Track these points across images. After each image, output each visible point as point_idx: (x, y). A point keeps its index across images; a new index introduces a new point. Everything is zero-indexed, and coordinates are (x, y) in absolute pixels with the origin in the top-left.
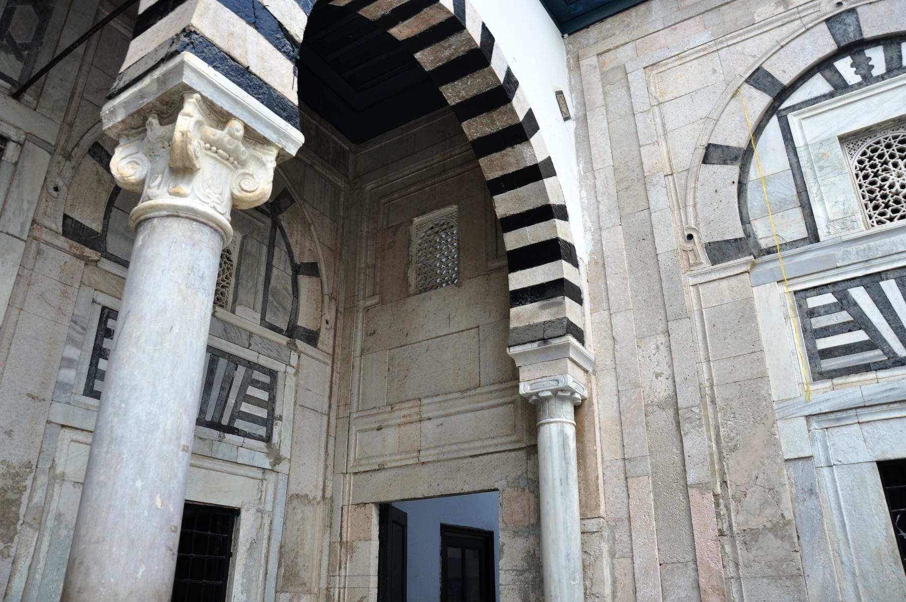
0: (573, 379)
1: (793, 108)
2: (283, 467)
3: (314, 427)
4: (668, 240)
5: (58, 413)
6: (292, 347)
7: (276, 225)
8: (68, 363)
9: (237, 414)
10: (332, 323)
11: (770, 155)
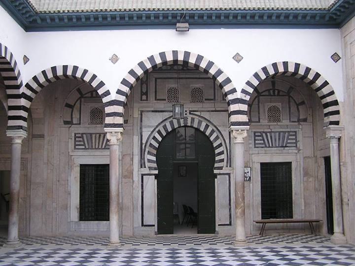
5: (251, 152)
6: (299, 124)
7: (290, 97)
8: (250, 143)
10: (311, 114)
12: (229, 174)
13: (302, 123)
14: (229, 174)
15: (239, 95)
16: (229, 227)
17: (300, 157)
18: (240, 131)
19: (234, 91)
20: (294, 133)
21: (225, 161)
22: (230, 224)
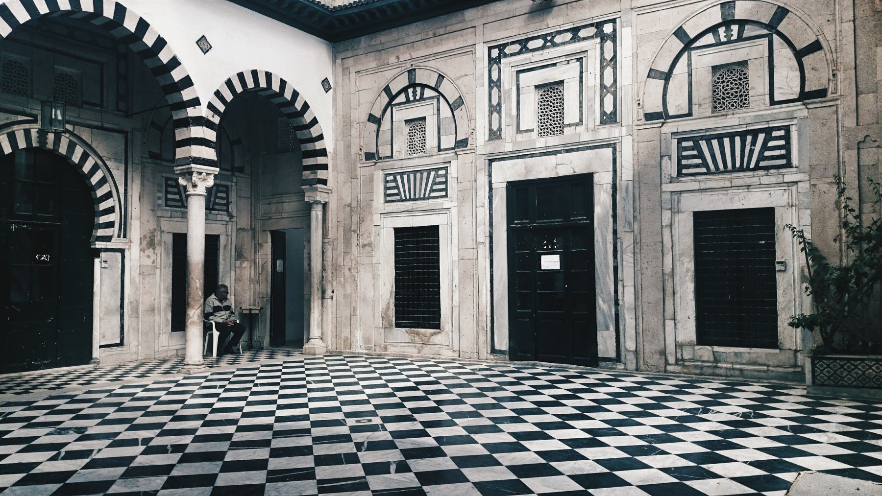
0: (320, 197)
1: (395, 105)
2: (234, 219)
3: (245, 204)
4: (355, 150)
5: (159, 213)
6: (233, 175)
8: (159, 198)
9: (215, 204)
11: (386, 125)
12: (122, 251)
13: (236, 174)
14: (122, 251)
15: (202, 111)
16: (119, 348)
17: (232, 228)
18: (204, 174)
19: (196, 102)
20: (225, 189)
21: (117, 225)
22: (121, 344)
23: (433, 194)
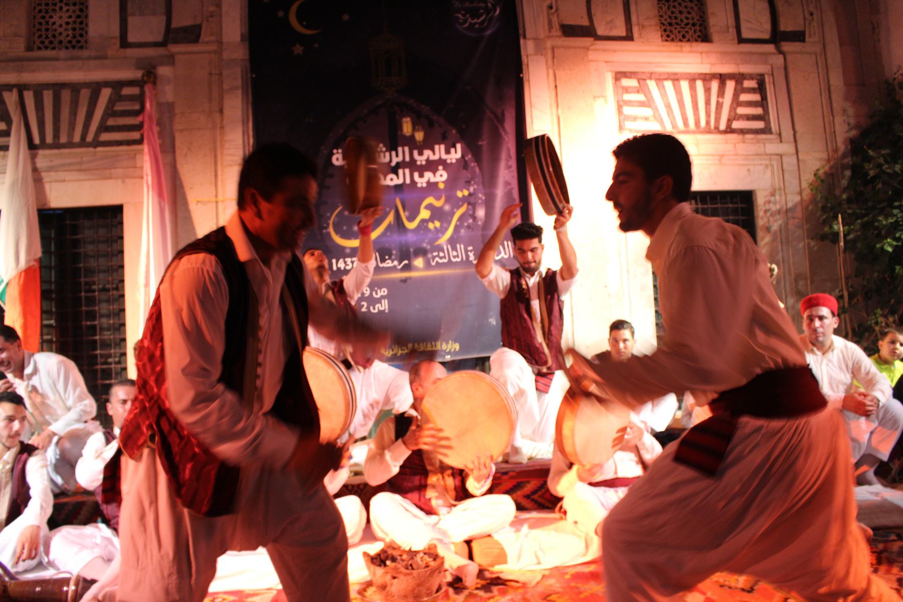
23: (105, 137)
